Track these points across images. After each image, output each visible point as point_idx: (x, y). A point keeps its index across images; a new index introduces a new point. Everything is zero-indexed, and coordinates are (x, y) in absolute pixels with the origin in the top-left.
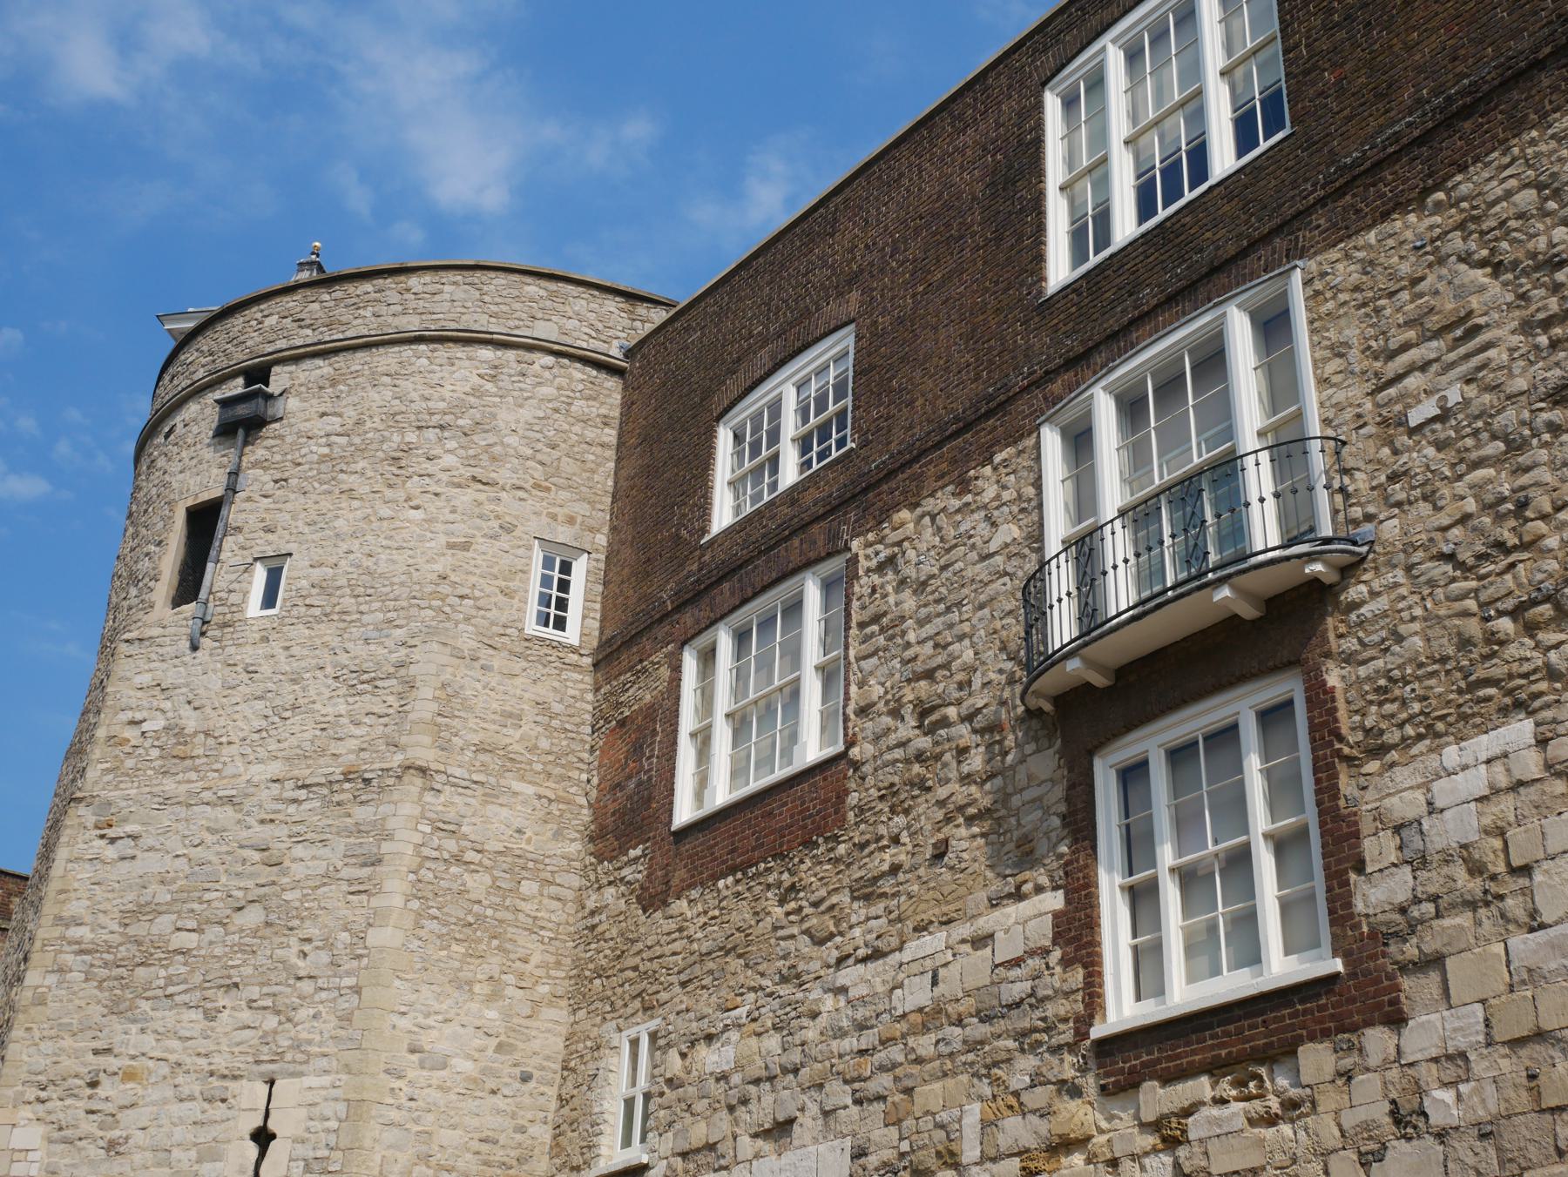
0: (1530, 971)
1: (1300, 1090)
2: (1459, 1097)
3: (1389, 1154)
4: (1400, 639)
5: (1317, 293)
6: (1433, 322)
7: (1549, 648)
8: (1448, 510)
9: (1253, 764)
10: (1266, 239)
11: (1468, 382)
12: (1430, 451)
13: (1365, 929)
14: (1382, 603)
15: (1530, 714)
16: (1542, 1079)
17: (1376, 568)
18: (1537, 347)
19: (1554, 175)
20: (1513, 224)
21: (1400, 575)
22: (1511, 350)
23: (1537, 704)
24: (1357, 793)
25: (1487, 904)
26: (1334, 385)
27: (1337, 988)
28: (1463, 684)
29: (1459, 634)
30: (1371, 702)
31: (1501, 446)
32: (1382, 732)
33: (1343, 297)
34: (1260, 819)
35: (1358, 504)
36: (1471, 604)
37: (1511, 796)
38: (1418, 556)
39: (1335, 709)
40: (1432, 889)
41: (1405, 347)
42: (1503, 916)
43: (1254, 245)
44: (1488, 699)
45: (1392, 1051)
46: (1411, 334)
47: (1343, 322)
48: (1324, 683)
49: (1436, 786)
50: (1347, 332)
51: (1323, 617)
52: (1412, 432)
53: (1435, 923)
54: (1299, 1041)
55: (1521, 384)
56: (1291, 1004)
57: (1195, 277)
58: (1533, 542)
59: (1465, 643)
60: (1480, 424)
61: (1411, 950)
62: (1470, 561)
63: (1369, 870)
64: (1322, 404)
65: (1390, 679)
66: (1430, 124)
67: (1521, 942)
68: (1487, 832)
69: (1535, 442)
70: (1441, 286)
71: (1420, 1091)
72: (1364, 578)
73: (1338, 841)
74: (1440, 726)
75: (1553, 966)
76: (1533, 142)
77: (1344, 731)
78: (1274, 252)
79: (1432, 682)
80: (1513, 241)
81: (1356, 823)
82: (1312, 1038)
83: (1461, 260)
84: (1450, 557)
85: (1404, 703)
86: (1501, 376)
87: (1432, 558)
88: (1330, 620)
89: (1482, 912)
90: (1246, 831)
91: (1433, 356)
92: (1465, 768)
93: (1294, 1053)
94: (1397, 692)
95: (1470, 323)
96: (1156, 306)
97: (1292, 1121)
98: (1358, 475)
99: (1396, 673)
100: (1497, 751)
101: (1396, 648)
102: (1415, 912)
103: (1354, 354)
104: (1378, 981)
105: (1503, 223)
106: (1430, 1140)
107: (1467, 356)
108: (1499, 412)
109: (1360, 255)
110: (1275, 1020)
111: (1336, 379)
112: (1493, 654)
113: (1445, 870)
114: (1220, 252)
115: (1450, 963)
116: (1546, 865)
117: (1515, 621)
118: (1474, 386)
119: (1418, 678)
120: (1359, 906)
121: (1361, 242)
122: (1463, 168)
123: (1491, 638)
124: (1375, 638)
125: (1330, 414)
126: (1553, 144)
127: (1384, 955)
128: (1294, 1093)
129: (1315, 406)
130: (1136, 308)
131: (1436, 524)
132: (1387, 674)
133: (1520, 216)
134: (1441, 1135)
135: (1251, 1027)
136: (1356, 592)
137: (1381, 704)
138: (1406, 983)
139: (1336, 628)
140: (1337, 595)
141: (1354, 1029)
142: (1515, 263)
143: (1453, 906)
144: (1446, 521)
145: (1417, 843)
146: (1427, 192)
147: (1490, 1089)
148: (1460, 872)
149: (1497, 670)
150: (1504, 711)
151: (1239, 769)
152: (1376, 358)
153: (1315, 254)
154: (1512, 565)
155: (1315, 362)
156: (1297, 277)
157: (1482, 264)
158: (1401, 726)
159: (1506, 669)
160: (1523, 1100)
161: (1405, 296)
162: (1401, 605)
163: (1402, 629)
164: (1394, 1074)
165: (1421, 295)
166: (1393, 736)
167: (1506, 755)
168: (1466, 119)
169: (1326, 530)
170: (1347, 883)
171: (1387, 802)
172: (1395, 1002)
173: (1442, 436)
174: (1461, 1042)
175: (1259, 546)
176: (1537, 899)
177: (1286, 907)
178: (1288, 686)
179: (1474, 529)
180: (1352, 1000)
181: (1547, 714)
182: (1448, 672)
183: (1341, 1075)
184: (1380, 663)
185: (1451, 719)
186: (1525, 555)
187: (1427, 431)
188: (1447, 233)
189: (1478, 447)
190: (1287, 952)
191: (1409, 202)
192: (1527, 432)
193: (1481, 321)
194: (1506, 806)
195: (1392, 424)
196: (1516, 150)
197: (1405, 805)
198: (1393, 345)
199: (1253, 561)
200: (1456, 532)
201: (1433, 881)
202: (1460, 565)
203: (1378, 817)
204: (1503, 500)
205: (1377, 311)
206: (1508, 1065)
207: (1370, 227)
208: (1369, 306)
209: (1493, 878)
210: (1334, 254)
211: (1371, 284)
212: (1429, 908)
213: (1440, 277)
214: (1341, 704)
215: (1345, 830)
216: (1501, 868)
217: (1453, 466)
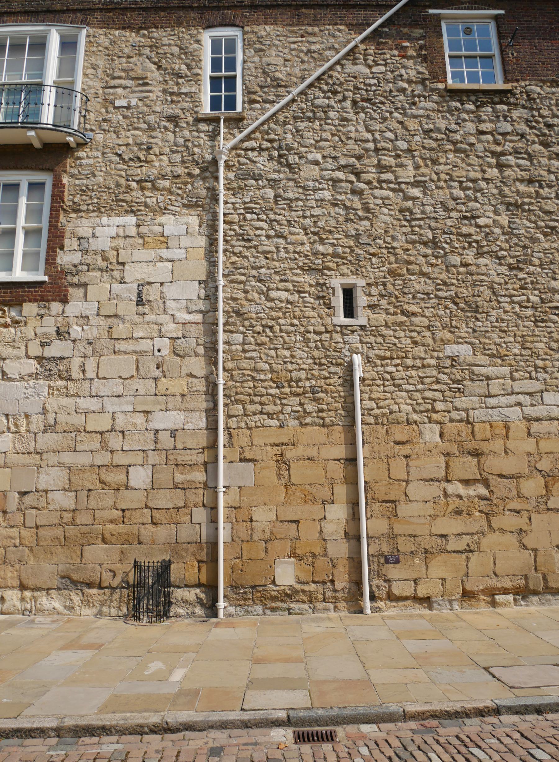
0: (117, 295)
1: (21, 318)
2: (83, 330)
3: (52, 344)
4: (94, 176)
5: (90, 42)
6: (132, 74)
7: (147, 197)
8: (122, 139)
9: (23, 201)
10: (75, 11)
11: (140, 100)
12: (121, 117)
13: (59, 269)
14: (91, 161)
15: (135, 215)
16: (114, 329)
17: (91, 149)
18: (166, 100)
19: (186, 47)
20: (168, 55)
21: (99, 155)
22: (158, 97)
23: (139, 213)
24: (66, 222)
25: (107, 271)
26: (88, 78)
27: (44, 286)
28: (114, 199)
29: (117, 182)
30: (78, 194)
31: (147, 127)
32: (80, 205)
33: (100, 48)
34: (21, 221)
35: (89, 124)
36: (123, 174)
37: (123, 239)
38: (108, 151)
39: (64, 191)
40: (88, 262)
41: (120, 78)
42: (112, 276)
43: (68, 11)
44: (122, 206)
45: (61, 311)
46: (123, 74)
47: (98, 57)
48: (62, 181)
49: (97, 229)
50: (99, 61)
51: (66, 158)
52: (115, 108)
53: (87, 273)
54: (25, 301)
55: (158, 109)
56: (24, 288)
57: (39, 9)
58: (150, 162)
59: (118, 185)
60: (141, 116)
61: (75, 280)
62: (127, 160)
63: (65, 249)
64: (83, 83)
65: (87, 188)
66: (149, 6)
67: (116, 286)
68: (112, 248)
69: (158, 130)
70: (139, 63)
71: (69, 325)
72: (86, 150)
73: (55, 237)
74: (103, 210)
75: (126, 295)
76: (182, 32)
77: (65, 200)
78: (76, 18)
79: (103, 194)
80: (167, 61)
81: (64, 233)
82: (30, 301)
83: (147, 58)
84: (120, 156)
85: (91, 198)
86: (152, 104)
87: (113, 153)
88: (68, 160)
89: (105, 273)
90: (15, 223)
91: (129, 85)
92: (109, 226)
93: (21, 305)
94: (89, 193)
95: (145, 81)
96: (19, 12)
97: (15, 328)
98: (91, 113)
99: (90, 187)
100: (122, 224)
101: (92, 179)
102: (80, 268)
103: (100, 71)
104: (60, 287)
105: (165, 53)
106: (69, 342)
107: (142, 91)
108: (148, 115)
109: (111, 37)
110: (16, 292)
111: (90, 76)
112: (127, 193)
113: (94, 257)
114: (53, 6)
115: (89, 287)
116: (130, 264)
117: (137, 184)
118: (141, 102)
119: (98, 191)
120: (59, 261)
121: (112, 32)
122: (157, 28)
123: (128, 187)
124: (85, 172)
125: (86, 88)
126: (189, 37)
127: (65, 279)
128: (18, 318)
129: (81, 82)
130: (9, 8)
131: (117, 142)
132: (87, 186)
133: (172, 54)
134: (74, 341)
135: (4, 293)
136: (81, 154)
137: (82, 195)
138: (71, 290)
139: (70, 164)
140: (73, 152)
141: (48, 301)
142: (166, 69)
143: (94, 269)
144: (121, 143)
145: (86, 245)
146: (141, 28)
147: (95, 329)
148: (99, 259)
149: (128, 198)
150: (127, 212)
151: (17, 200)
152: (108, 76)
153: (93, 27)
154: (141, 166)
155: (84, 66)
156: (84, 32)
157: (155, 63)
158: (88, 205)
159: (131, 199)
160: (106, 334)
161: (124, 60)
162: (97, 165)
163: (96, 173)
164: (60, 318)
165: (130, 63)
166: (84, 208)
167: (124, 226)
168: (163, 11)
169: (76, 128)
170: (56, 252)
171: (77, 229)
172: (66, 295)
173: (126, 114)
174: (88, 313)
175: (45, 122)
176: (125, 274)
177: (25, 254)
178: (47, 178)
179: (130, 150)
180: (49, 292)
181: (142, 218)
182: (110, 193)
183: (39, 315)
184: (85, 181)
185: (107, 209)
186: (146, 165)
187: (121, 110)
188: (145, 46)
189: (138, 123)
190: (22, 270)
191: (134, 28)
192: (156, 126)
193: (150, 82)
194: (120, 242)
195: (108, 102)
196: (176, 32)
197: (84, 231)
198: (116, 74)
199: (42, 126)
200: (123, 148)
201: (89, 259)
202: (123, 160)
203: (73, 233)
204: (143, 144)
205: (112, 60)
206: (102, 322)
207: (117, 29)
208: (110, 57)
209: (111, 263)
210: (101, 31)
211: (112, 49)
212: (86, 268)
213: (139, 60)
214: (66, 190)
215: (59, 234)
216: (114, 261)
217: (128, 126)
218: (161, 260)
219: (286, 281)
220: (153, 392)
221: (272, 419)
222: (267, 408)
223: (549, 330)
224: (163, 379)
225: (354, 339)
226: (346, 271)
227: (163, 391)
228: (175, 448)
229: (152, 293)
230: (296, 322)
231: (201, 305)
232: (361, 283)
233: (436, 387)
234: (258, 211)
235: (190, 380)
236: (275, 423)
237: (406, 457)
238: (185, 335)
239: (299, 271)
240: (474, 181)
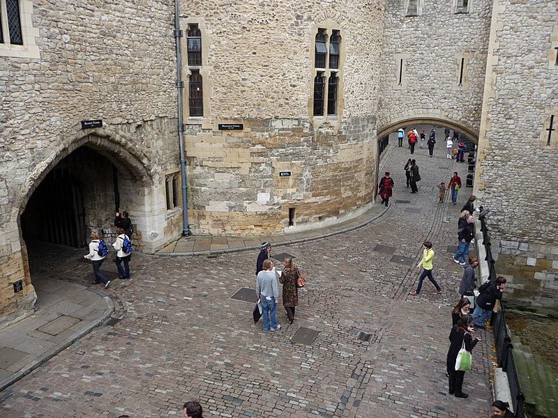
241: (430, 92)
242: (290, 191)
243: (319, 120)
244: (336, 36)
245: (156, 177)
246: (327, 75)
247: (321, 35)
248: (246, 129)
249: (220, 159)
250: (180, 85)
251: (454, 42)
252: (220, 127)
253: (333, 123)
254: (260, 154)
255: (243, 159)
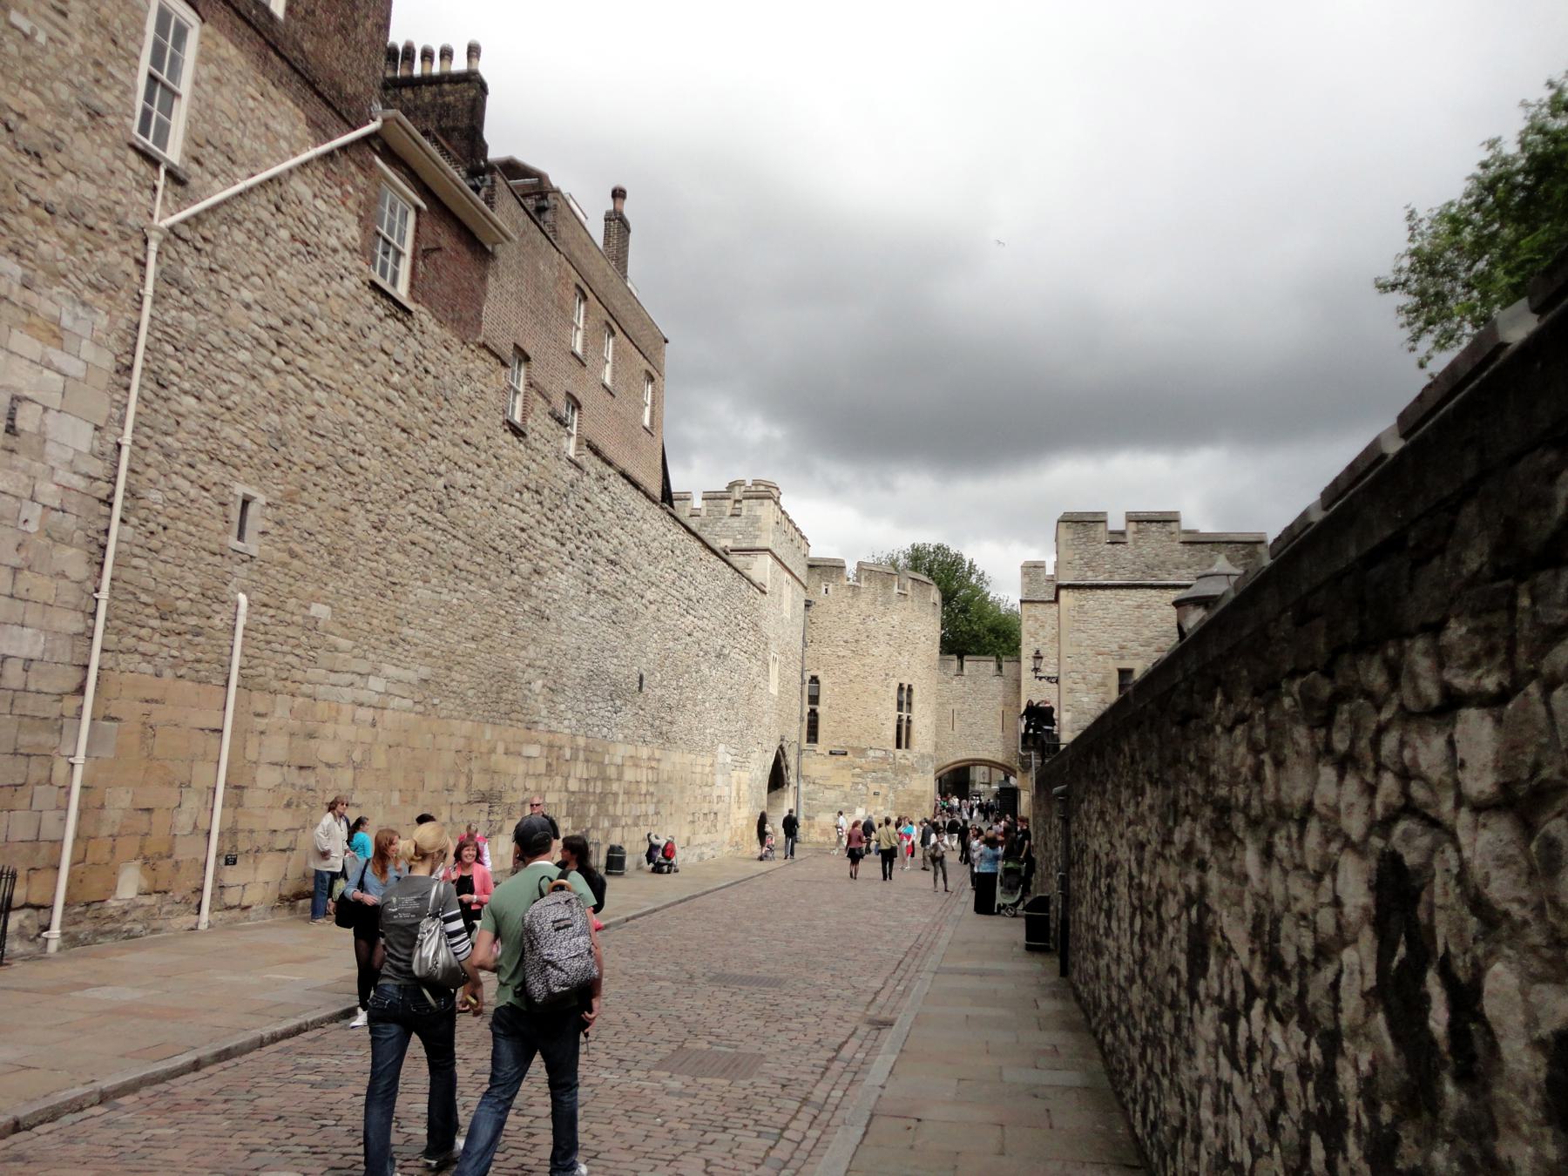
218: (48, 366)
219: (191, 466)
220: (7, 591)
221: (149, 662)
222: (142, 647)
223: (386, 607)
224: (26, 572)
225: (242, 570)
226: (251, 477)
227: (23, 594)
228: (25, 690)
229: (27, 419)
230: (192, 529)
231: (98, 468)
232: (262, 499)
233: (296, 652)
234: (179, 345)
235: (62, 582)
236: (149, 669)
237: (262, 733)
238: (65, 508)
239: (205, 457)
240: (366, 408)
241: (978, 737)
242: (880, 808)
243: (899, 753)
244: (910, 689)
245: (791, 787)
246: (905, 718)
247: (901, 687)
248: (850, 755)
249: (828, 778)
250: (802, 720)
251: (994, 697)
252: (831, 753)
253: (909, 756)
254: (859, 776)
255: (845, 779)
